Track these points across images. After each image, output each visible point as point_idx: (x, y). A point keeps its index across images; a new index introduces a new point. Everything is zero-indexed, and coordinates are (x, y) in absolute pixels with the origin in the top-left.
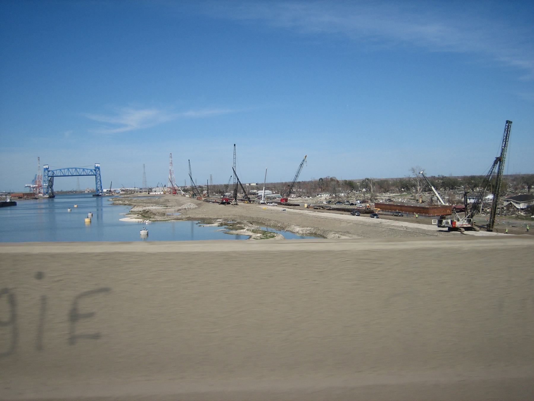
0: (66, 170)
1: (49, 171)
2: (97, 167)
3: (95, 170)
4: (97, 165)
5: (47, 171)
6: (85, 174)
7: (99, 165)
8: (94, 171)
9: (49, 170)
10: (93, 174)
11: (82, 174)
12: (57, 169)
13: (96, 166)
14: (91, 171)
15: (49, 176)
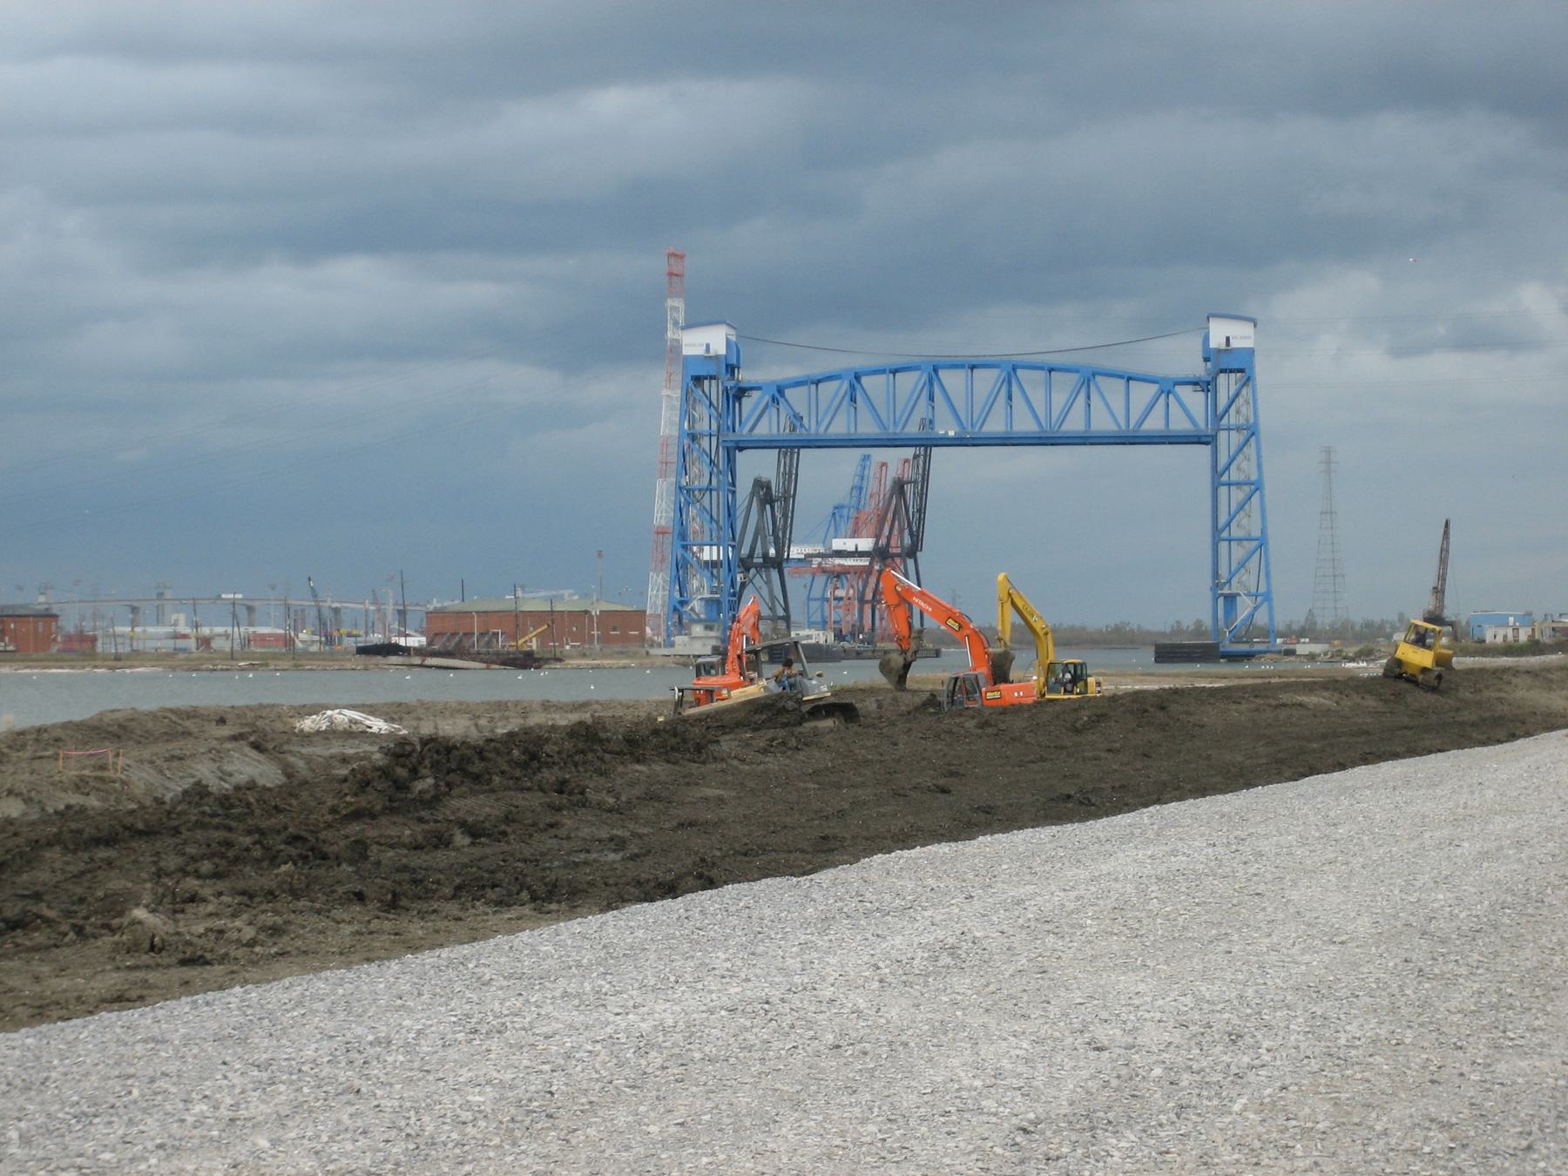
0: (907, 381)
1: (741, 393)
2: (1228, 350)
3: (1205, 386)
4: (1219, 333)
5: (713, 389)
6: (1102, 423)
7: (1241, 335)
8: (1195, 400)
9: (745, 376)
10: (1180, 424)
11: (1075, 424)
12: (817, 370)
13: (1216, 341)
14: (1167, 387)
15: (743, 432)
